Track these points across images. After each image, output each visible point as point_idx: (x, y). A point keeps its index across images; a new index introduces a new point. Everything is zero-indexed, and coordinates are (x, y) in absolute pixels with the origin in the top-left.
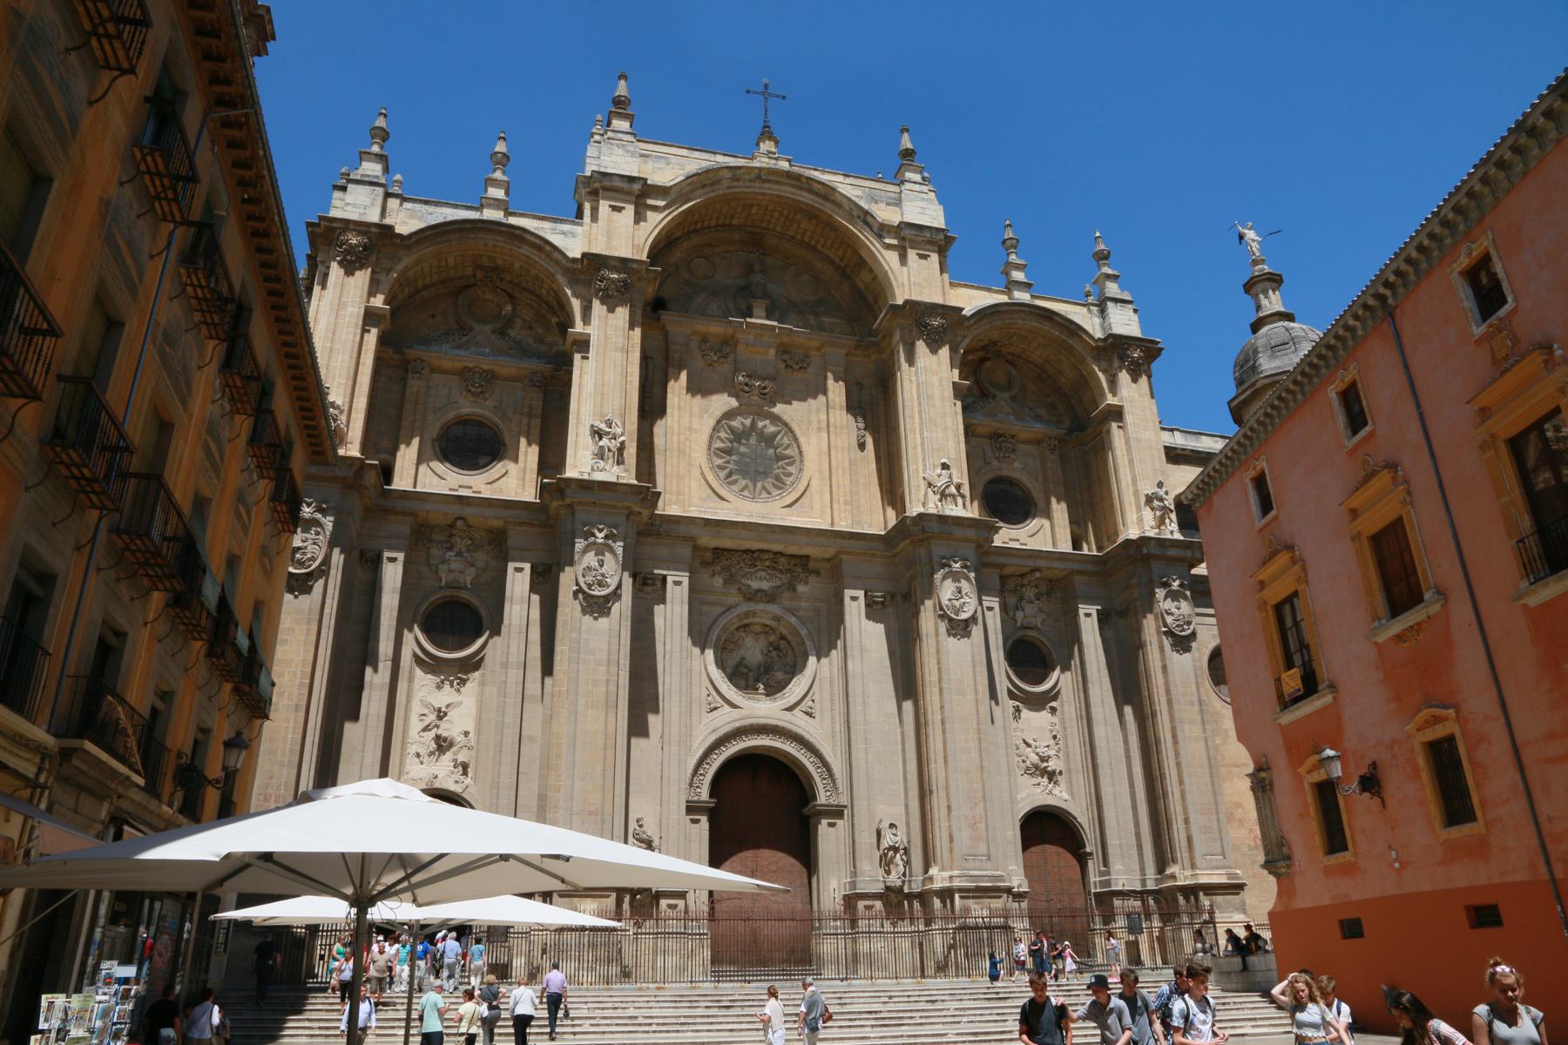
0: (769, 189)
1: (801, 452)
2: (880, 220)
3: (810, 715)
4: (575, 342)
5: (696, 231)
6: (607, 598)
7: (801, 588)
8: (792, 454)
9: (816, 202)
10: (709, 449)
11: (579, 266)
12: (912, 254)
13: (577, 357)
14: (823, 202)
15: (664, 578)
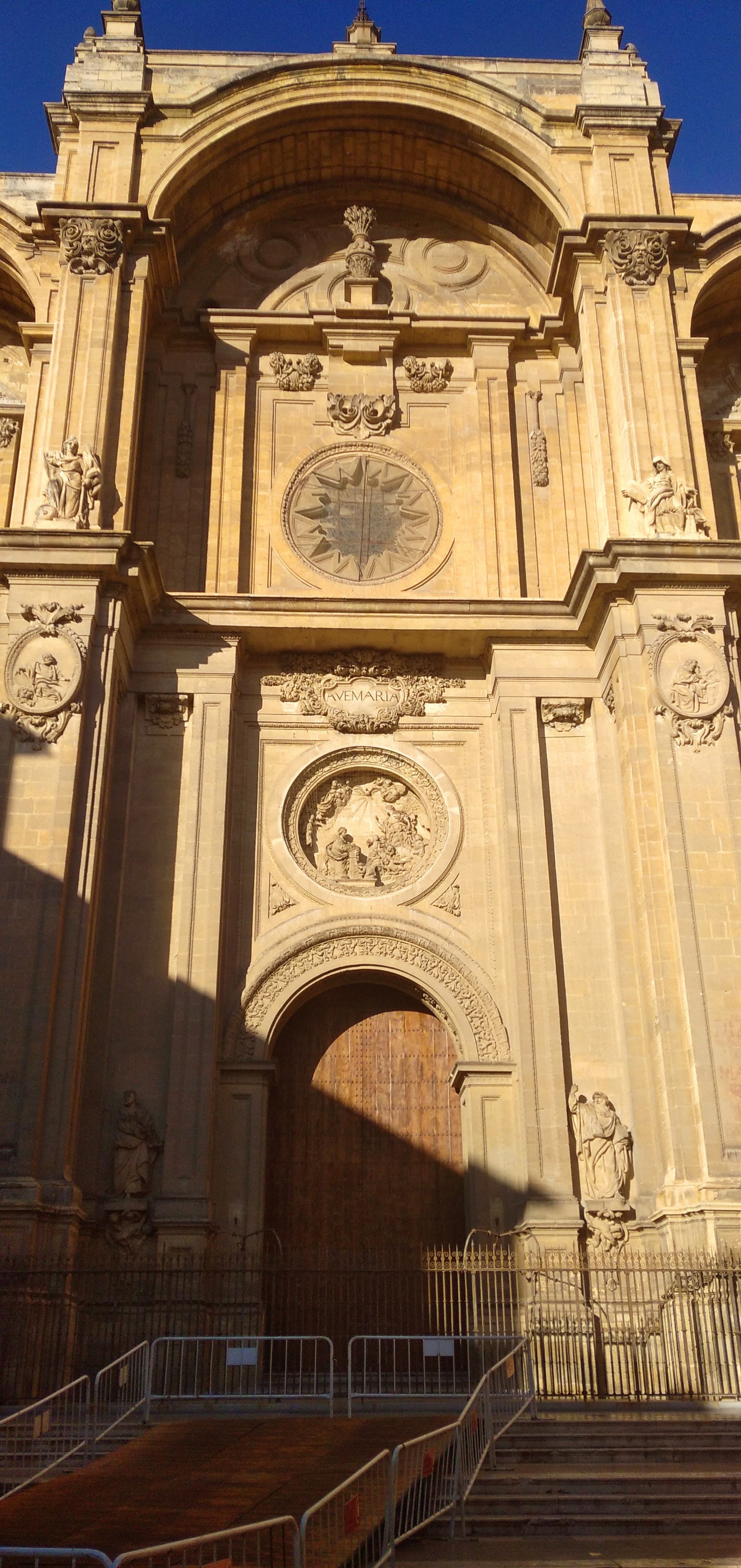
0: (356, 94)
1: (438, 509)
2: (544, 112)
3: (454, 910)
4: (33, 340)
5: (264, 195)
6: (54, 714)
7: (430, 708)
8: (426, 510)
9: (438, 103)
10: (286, 509)
11: (39, 227)
12: (600, 160)
13: (37, 363)
14: (449, 101)
15: (191, 697)
